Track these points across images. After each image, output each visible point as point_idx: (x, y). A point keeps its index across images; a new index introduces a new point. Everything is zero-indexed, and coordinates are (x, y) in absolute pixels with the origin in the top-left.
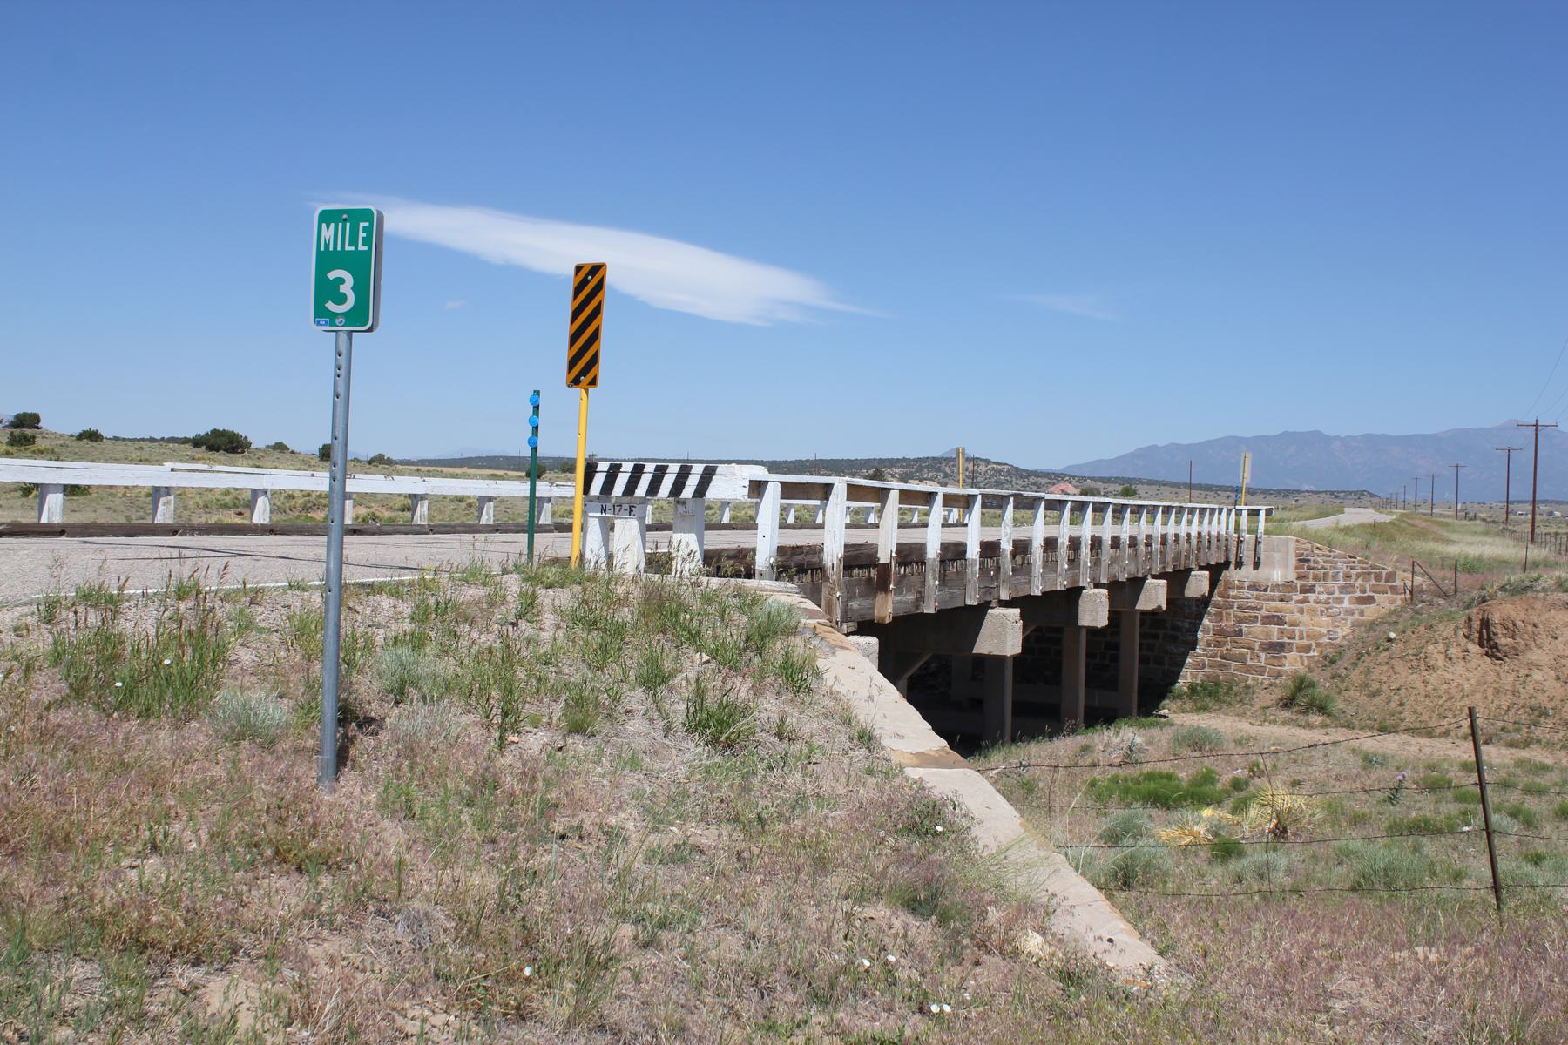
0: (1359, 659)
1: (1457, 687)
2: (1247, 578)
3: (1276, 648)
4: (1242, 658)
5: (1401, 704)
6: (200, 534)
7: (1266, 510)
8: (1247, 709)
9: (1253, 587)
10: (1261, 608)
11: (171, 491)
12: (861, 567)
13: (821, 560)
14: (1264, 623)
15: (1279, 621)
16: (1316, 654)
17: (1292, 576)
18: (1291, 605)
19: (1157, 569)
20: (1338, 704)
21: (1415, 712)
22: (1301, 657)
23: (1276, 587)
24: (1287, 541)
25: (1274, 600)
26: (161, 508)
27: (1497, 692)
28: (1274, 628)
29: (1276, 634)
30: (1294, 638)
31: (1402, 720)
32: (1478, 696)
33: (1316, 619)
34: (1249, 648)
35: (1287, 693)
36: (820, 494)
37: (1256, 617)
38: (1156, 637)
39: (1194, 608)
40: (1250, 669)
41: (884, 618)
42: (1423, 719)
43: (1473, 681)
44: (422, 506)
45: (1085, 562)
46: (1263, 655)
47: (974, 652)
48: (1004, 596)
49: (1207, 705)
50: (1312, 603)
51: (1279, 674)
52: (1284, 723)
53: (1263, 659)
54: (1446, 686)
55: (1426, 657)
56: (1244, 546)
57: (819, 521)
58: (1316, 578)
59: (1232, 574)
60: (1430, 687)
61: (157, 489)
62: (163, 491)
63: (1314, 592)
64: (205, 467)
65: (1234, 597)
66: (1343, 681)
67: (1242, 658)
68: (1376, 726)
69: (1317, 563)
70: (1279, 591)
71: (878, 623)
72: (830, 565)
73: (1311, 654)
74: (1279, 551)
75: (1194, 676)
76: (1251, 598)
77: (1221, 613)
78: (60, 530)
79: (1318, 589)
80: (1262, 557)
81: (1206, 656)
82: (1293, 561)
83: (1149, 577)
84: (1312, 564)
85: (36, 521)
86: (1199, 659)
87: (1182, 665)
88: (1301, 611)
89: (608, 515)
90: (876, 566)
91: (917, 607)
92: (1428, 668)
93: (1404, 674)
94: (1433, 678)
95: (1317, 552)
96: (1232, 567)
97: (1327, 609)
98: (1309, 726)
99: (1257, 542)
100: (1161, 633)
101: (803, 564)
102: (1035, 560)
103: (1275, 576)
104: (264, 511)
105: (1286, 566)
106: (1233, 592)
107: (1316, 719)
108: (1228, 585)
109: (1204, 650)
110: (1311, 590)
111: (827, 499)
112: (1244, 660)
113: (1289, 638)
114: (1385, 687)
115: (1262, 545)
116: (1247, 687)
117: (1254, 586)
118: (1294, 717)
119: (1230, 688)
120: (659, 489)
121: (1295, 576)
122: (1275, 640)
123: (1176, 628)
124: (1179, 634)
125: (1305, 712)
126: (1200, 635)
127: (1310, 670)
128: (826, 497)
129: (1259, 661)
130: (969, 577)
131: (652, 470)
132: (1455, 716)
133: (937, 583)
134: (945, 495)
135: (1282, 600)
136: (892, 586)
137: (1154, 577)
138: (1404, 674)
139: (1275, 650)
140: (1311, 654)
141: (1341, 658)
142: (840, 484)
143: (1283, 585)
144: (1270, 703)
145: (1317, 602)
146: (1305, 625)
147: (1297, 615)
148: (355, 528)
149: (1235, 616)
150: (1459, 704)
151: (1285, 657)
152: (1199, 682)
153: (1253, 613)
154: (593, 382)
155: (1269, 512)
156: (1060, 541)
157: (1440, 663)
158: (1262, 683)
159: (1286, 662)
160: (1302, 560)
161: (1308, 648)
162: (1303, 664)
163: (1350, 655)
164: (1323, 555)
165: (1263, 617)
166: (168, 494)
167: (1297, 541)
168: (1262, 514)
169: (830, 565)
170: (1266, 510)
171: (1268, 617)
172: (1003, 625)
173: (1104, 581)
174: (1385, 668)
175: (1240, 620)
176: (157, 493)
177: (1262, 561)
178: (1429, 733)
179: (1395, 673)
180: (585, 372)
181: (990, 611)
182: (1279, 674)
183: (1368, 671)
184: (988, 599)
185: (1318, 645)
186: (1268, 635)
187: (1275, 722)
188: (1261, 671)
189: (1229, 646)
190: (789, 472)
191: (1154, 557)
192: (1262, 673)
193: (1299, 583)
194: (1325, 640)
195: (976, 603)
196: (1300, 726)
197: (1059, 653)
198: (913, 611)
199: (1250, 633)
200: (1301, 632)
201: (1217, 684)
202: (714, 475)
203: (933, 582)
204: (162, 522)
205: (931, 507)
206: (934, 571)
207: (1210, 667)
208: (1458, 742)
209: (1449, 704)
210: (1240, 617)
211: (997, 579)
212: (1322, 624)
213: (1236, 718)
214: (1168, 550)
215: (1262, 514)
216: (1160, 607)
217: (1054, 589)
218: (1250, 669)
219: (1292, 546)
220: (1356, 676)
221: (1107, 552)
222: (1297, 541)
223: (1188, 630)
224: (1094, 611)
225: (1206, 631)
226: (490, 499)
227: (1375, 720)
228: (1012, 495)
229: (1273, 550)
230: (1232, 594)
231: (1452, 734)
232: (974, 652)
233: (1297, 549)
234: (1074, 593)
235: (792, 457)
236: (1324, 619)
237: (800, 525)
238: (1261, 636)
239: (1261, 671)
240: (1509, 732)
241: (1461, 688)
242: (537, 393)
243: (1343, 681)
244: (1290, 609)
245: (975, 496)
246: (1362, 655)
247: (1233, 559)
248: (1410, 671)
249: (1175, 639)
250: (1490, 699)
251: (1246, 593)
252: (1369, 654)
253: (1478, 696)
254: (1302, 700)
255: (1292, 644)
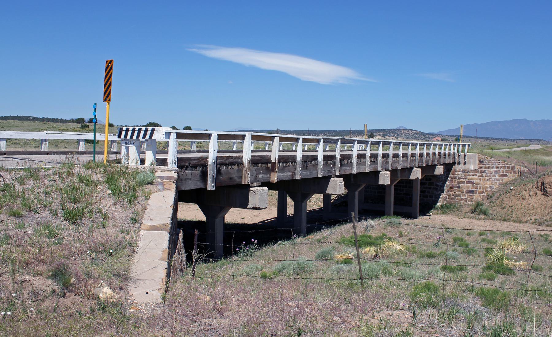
0: (500, 196)
1: (532, 206)
2: (462, 168)
3: (471, 192)
4: (459, 196)
5: (512, 212)
6: (57, 154)
7: (468, 144)
8: (460, 213)
9: (463, 171)
10: (466, 178)
11: (47, 140)
12: (263, 163)
13: (242, 161)
14: (467, 184)
15: (472, 183)
16: (485, 194)
17: (477, 167)
18: (477, 177)
19: (417, 165)
20: (490, 211)
21: (516, 214)
22: (480, 195)
23: (471, 171)
24: (475, 156)
25: (470, 176)
26: (43, 146)
27: (546, 207)
28: (471, 185)
29: (471, 187)
30: (477, 189)
31: (512, 217)
32: (539, 209)
33: (485, 182)
34: (462, 192)
35: (473, 208)
36: (241, 138)
37: (464, 182)
38: (430, 188)
39: (443, 179)
40: (462, 199)
41: (273, 181)
42: (519, 217)
43: (538, 204)
44: (144, 145)
45: (380, 162)
46: (466, 195)
47: (326, 193)
48: (337, 174)
49: (446, 212)
50: (484, 177)
51: (472, 201)
52: (471, 218)
53: (466, 196)
54: (528, 205)
55: (522, 195)
56: (460, 157)
57: (317, 149)
58: (486, 168)
59: (456, 167)
60: (523, 206)
61: (42, 140)
62: (43, 140)
63: (485, 173)
64: (59, 132)
65: (457, 175)
66: (493, 203)
67: (459, 196)
68: (502, 219)
69: (486, 163)
70: (472, 173)
71: (272, 183)
72: (245, 162)
73: (484, 194)
74: (472, 159)
75: (443, 202)
76: (463, 175)
77: (452, 180)
78: (4, 153)
79: (486, 172)
80: (467, 161)
81: (447, 195)
82: (477, 162)
83: (414, 167)
84: (484, 163)
85: (40, 150)
86: (445, 196)
87: (439, 198)
88: (480, 179)
89: (127, 145)
90: (271, 163)
91: (293, 177)
92: (523, 199)
93: (514, 201)
94: (524, 203)
95: (486, 159)
96: (456, 164)
97: (490, 179)
98: (479, 219)
99: (465, 156)
100: (432, 187)
101: (233, 162)
102: (354, 162)
103: (471, 167)
104: (83, 147)
105: (475, 164)
106: (457, 173)
107: (482, 216)
108: (455, 171)
109: (447, 193)
110: (484, 172)
111: (244, 140)
112: (460, 196)
113: (475, 189)
114: (507, 206)
115: (467, 157)
116: (461, 206)
117: (464, 171)
118: (475, 216)
119: (455, 206)
120: (146, 137)
121: (478, 167)
122: (471, 189)
123: (437, 185)
124: (438, 187)
125: (478, 214)
126: (445, 188)
127: (483, 200)
128: (210, 138)
129: (465, 197)
130: (319, 167)
131: (138, 130)
132: (530, 216)
133: (300, 169)
134: (303, 139)
135: (473, 176)
136: (276, 170)
137: (417, 168)
138: (514, 201)
139: (470, 193)
140: (484, 194)
141: (494, 196)
142: (248, 135)
143: (474, 170)
144: (467, 211)
145: (486, 176)
146: (481, 184)
147: (479, 181)
148: (117, 152)
149: (457, 181)
150: (532, 212)
151: (474, 195)
152: (444, 204)
153: (463, 180)
154: (110, 100)
155: (469, 145)
156: (367, 155)
157: (527, 197)
158: (466, 204)
159: (474, 197)
160: (481, 162)
161: (482, 192)
162: (480, 198)
163: (497, 195)
164: (488, 160)
165: (467, 182)
166: (46, 141)
167: (479, 155)
168: (467, 146)
169: (245, 162)
170: (468, 144)
171: (468, 181)
172: (336, 184)
173: (390, 169)
174: (508, 199)
175: (459, 183)
176: (43, 141)
177: (466, 162)
178: (520, 222)
179: (512, 201)
180: (107, 97)
181: (331, 179)
182: (472, 201)
183: (502, 200)
184: (330, 174)
185: (486, 191)
186: (468, 188)
187: (468, 218)
188: (466, 200)
189: (455, 191)
190: (309, 135)
191: (416, 161)
192: (466, 201)
193: (479, 170)
194: (489, 189)
195: (321, 176)
196: (476, 219)
197: (385, 193)
198: (291, 179)
199: (462, 187)
200: (480, 187)
201: (451, 205)
202: (154, 131)
203: (299, 168)
204: (44, 150)
205: (298, 143)
206: (299, 165)
207: (449, 198)
208: (530, 225)
209: (528, 211)
210: (459, 181)
211: (334, 168)
212: (488, 184)
213: (455, 216)
214: (424, 158)
215: (467, 146)
216: (418, 178)
217: (364, 171)
218: (462, 199)
219: (477, 157)
220: (498, 202)
221: (391, 160)
222: (479, 155)
223: (441, 186)
224: (385, 179)
225: (447, 186)
226: (46, 140)
227: (502, 217)
228: (340, 139)
229: (470, 158)
230: (456, 173)
231: (528, 222)
232: (326, 193)
233: (479, 158)
234: (376, 173)
235: (306, 129)
236: (489, 182)
237: (309, 150)
238: (466, 188)
239: (466, 200)
240: (548, 221)
241: (533, 206)
242: (96, 104)
243: (493, 203)
244: (476, 179)
245: (320, 139)
246: (501, 195)
247: (456, 161)
248: (517, 200)
249: (437, 189)
250: (543, 210)
251: (461, 173)
252: (504, 194)
253: (539, 209)
254: (478, 210)
255: (477, 191)
